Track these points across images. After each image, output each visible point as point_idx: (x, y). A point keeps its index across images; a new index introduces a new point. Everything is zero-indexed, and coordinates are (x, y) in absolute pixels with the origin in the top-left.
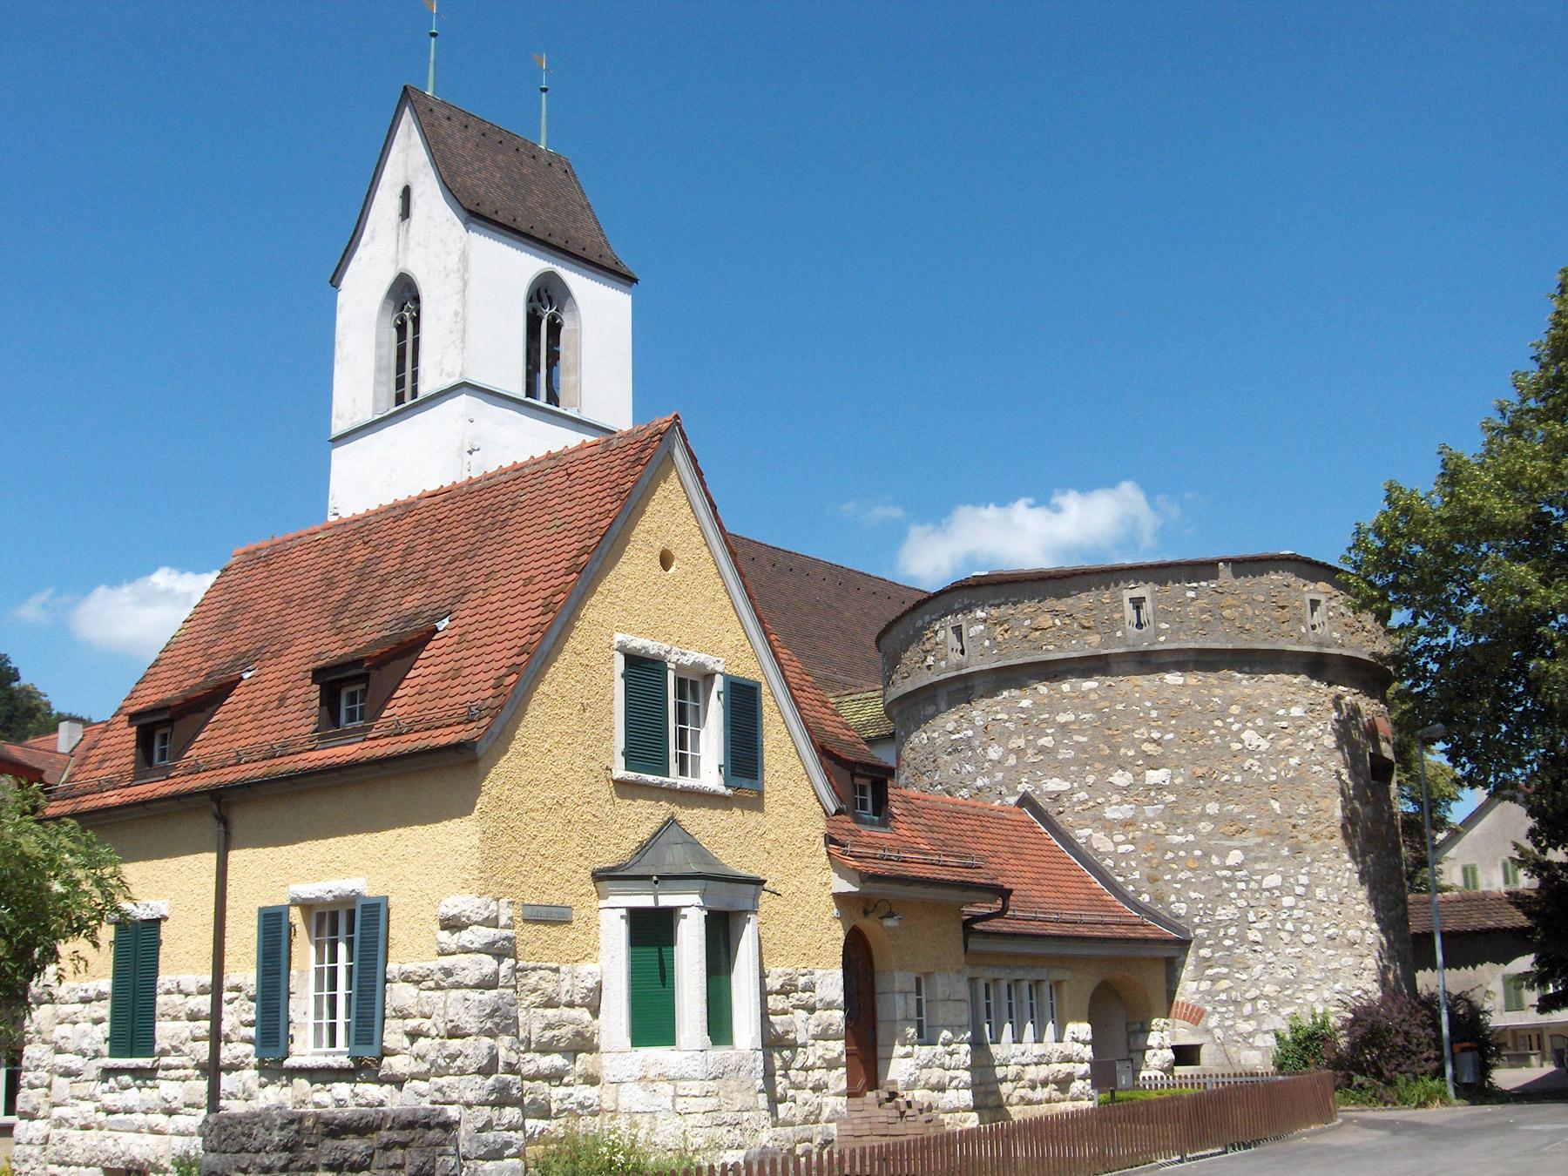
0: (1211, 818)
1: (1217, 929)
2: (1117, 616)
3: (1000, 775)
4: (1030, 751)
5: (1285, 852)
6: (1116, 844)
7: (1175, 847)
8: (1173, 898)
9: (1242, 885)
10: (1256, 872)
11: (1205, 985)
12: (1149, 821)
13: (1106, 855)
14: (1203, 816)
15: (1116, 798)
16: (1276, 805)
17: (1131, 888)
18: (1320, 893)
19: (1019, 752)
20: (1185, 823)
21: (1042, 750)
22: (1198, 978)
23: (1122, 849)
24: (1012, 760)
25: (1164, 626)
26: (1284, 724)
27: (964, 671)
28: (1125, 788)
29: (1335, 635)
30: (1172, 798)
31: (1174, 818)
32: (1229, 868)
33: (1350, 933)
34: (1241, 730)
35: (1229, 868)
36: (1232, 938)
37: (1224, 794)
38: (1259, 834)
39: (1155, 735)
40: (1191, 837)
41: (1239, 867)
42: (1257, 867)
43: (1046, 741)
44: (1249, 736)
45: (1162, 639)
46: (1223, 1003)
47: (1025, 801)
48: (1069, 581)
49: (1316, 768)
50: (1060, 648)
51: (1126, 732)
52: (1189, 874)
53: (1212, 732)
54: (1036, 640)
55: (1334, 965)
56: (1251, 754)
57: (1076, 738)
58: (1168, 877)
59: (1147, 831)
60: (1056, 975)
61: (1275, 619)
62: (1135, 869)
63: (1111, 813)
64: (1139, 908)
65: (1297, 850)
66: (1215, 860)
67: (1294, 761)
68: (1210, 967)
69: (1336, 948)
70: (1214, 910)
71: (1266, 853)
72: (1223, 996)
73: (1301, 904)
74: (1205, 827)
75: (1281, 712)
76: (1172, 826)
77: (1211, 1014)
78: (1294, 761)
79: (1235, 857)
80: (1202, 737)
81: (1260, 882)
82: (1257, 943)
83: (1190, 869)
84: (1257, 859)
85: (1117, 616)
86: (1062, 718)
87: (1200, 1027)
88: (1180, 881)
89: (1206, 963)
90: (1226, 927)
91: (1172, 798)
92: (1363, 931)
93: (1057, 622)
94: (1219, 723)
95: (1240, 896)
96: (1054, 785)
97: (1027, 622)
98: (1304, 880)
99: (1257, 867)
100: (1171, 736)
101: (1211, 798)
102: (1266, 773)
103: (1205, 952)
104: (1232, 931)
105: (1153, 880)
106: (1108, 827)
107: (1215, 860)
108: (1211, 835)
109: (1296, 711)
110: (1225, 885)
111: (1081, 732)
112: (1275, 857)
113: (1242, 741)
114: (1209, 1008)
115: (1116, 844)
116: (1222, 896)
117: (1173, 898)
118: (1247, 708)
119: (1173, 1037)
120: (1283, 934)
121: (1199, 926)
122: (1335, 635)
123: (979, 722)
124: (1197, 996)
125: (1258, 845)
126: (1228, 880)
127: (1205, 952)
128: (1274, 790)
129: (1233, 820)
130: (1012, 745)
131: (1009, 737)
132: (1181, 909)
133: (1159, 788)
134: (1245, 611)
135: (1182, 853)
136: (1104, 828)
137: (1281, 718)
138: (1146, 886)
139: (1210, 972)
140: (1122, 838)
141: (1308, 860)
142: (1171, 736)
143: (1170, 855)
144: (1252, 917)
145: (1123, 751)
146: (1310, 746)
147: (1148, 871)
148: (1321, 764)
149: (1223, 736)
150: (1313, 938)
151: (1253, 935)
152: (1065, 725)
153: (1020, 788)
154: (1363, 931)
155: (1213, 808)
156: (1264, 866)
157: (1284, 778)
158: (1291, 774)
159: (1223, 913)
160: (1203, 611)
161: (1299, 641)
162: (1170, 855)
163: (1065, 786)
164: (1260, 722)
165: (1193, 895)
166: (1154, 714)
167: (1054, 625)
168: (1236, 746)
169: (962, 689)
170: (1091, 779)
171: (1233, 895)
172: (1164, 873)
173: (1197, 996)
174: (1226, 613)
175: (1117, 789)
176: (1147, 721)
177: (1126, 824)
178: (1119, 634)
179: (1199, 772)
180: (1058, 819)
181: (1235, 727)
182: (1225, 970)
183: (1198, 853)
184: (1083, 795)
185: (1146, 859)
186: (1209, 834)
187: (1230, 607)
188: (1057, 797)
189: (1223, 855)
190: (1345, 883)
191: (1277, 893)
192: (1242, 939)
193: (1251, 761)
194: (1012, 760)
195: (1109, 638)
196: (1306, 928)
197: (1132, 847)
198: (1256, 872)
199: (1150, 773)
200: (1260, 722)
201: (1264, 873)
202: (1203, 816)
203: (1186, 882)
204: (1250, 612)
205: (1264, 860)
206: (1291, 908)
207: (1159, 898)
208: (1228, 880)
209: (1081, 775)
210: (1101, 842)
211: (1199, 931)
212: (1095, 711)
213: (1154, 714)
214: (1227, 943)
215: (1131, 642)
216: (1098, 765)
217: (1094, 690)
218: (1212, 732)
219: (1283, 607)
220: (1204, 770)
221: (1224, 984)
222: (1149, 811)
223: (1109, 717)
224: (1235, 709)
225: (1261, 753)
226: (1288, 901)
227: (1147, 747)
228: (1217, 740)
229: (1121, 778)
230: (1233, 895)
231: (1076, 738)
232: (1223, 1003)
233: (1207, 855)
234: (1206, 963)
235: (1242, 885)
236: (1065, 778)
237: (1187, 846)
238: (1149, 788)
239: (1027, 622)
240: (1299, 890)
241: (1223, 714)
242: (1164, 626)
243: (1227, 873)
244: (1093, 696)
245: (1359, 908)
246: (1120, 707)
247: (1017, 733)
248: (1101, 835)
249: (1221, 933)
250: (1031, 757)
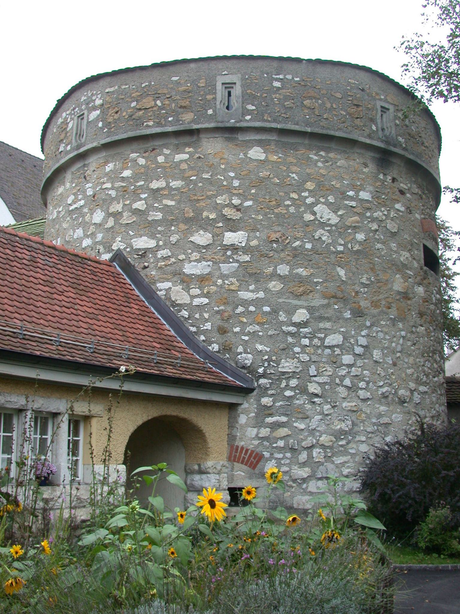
0: (281, 278)
1: (280, 380)
2: (209, 97)
3: (99, 237)
4: (125, 214)
5: (348, 315)
6: (193, 297)
7: (246, 303)
8: (240, 349)
9: (306, 342)
10: (320, 330)
11: (265, 432)
12: (224, 277)
13: (181, 306)
14: (274, 275)
15: (195, 255)
16: (342, 272)
17: (202, 338)
18: (377, 354)
19: (117, 215)
20: (257, 281)
21: (137, 212)
22: (259, 423)
23: (197, 302)
24: (111, 223)
25: (251, 107)
26: (353, 204)
27: (82, 150)
28: (204, 247)
29: (400, 139)
30: (247, 258)
31: (250, 275)
32: (294, 324)
33: (401, 392)
34: (314, 204)
35: (294, 324)
36: (293, 389)
37: (297, 255)
38: (325, 297)
39: (236, 201)
40: (261, 295)
41: (305, 324)
42: (321, 325)
43: (139, 205)
44: (323, 212)
45: (248, 118)
46: (280, 450)
47: (118, 256)
48: (172, 69)
49: (379, 246)
50: (159, 124)
51: (209, 197)
52: (257, 328)
53: (288, 203)
54: (140, 118)
55: (385, 420)
56: (323, 225)
57: (165, 202)
58: (237, 329)
59: (221, 287)
60: (81, 408)
61: (350, 114)
62: (207, 321)
63: (189, 269)
64: (208, 355)
65: (358, 313)
66: (282, 317)
67: (360, 237)
68: (271, 415)
69: (388, 405)
70: (278, 363)
71: (329, 313)
72: (281, 443)
73: (359, 363)
74: (275, 286)
75: (351, 193)
76: (243, 285)
77: (269, 459)
78: (360, 237)
79: (301, 315)
80: (278, 206)
81: (322, 340)
82: (317, 395)
83: (258, 324)
84: (321, 318)
85: (209, 97)
86: (155, 185)
87: (257, 471)
88: (249, 334)
89: (267, 411)
90: (288, 379)
91: (247, 258)
92: (412, 391)
93: (159, 103)
94: (294, 196)
95: (303, 352)
96: (143, 242)
97: (133, 104)
98: (363, 341)
99: (321, 325)
100: (249, 203)
101: (282, 261)
102: (334, 243)
103: (266, 401)
104: (293, 382)
105: (222, 331)
106: (186, 281)
107: (282, 317)
108: (280, 293)
109: (364, 195)
110: (290, 339)
111: (170, 197)
112: (338, 318)
113: (314, 214)
114: (267, 454)
115: (193, 297)
116: (286, 350)
117: (240, 349)
118: (320, 186)
119: (231, 478)
120: (341, 389)
121: (264, 375)
122: (400, 139)
123: (90, 192)
124: (256, 442)
125: (323, 306)
126: (292, 335)
127: (266, 401)
128: (341, 259)
129: (301, 280)
130: (112, 210)
131: (111, 203)
132: (248, 359)
133: (234, 248)
134: (324, 103)
135: (252, 309)
136: (183, 281)
137: (351, 198)
138: (215, 337)
139: (269, 420)
140: (197, 291)
141: (368, 324)
142: (249, 203)
143: (240, 309)
144: (312, 371)
145: (205, 214)
146: (375, 226)
147: (220, 323)
148: (383, 243)
149: (298, 207)
150: (368, 395)
151: (313, 388)
152: (158, 190)
153: (115, 247)
154: (412, 391)
155: (283, 270)
156: (328, 325)
157: (351, 251)
158: (357, 247)
159: (287, 365)
160: (286, 98)
161: (369, 136)
162: (240, 309)
163: (152, 244)
164: (331, 199)
165: (260, 347)
166: (236, 183)
167: (156, 105)
168: (308, 217)
169: (192, 288)
170: (174, 239)
171: (297, 349)
172: (234, 326)
173: (256, 442)
174: (307, 102)
175: (198, 247)
176: (229, 190)
177: (202, 279)
178: (210, 112)
179: (274, 236)
180: (142, 273)
181: (309, 201)
182: (284, 419)
183: (267, 309)
184: (165, 252)
185: (218, 312)
186: (278, 292)
187: (310, 98)
188: (144, 254)
189: (291, 312)
190: (399, 348)
191: (338, 351)
192: (303, 390)
193: (321, 231)
194: (111, 223)
195: (201, 115)
196: (362, 384)
197: (206, 301)
198: (320, 330)
199: (228, 235)
200: (331, 199)
201: (327, 332)
202: (274, 275)
203: (254, 334)
204: (328, 105)
205: (328, 319)
206: (350, 366)
207: (226, 348)
208: (292, 335)
209: (167, 234)
210: (180, 295)
211: (262, 381)
212: (183, 179)
213: (236, 183)
214: (288, 393)
215: (220, 119)
216: (182, 226)
217: (185, 161)
218: (288, 203)
219: (358, 106)
220: (278, 235)
221: (283, 432)
222: (225, 268)
223: (195, 184)
224: (310, 185)
225: (331, 225)
226: (347, 359)
227: (227, 211)
228: (292, 210)
229: (202, 238)
230: (297, 349)
231: (165, 202)
232: (280, 450)
233: (275, 312)
234: (267, 411)
235: (306, 342)
236: (152, 236)
237: (257, 302)
238: (226, 248)
239: (133, 104)
240: (358, 350)
241: (300, 187)
242: (251, 107)
243: (291, 329)
244: (184, 166)
245: (409, 371)
246: (206, 176)
247: (116, 199)
248: (179, 288)
249: (283, 384)
250: (126, 218)
